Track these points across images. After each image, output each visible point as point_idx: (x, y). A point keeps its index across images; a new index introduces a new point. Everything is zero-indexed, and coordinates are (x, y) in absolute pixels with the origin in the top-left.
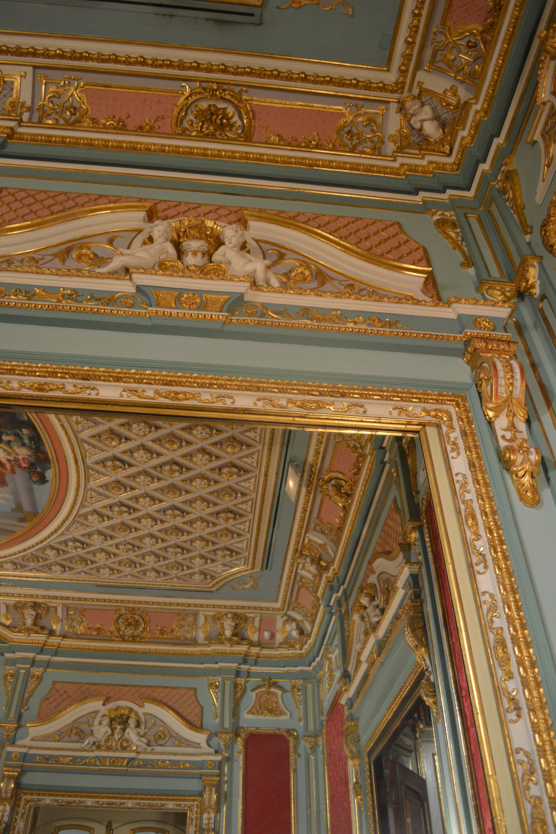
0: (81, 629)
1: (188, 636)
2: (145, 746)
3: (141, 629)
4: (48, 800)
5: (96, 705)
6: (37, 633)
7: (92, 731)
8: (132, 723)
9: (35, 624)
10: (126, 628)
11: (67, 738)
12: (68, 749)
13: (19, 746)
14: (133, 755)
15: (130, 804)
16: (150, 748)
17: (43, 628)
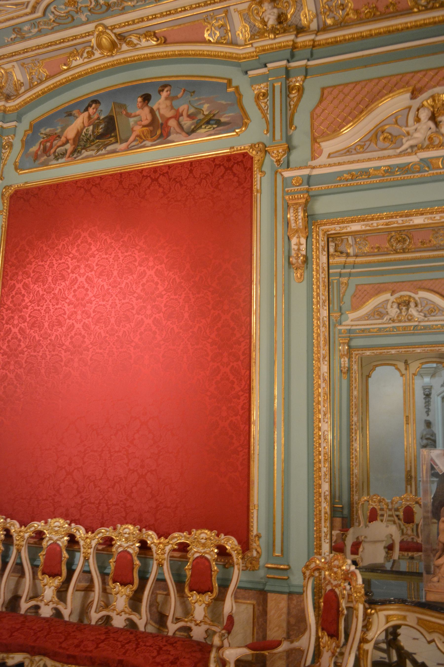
0: (366, 249)
2: (423, 318)
3: (407, 243)
4: (368, 353)
5: (387, 296)
6: (339, 256)
7: (387, 312)
8: (412, 304)
9: (336, 251)
10: (397, 244)
11: (372, 318)
12: (375, 324)
13: (344, 325)
14: (416, 323)
15: (419, 350)
16: (426, 319)
17: (342, 253)
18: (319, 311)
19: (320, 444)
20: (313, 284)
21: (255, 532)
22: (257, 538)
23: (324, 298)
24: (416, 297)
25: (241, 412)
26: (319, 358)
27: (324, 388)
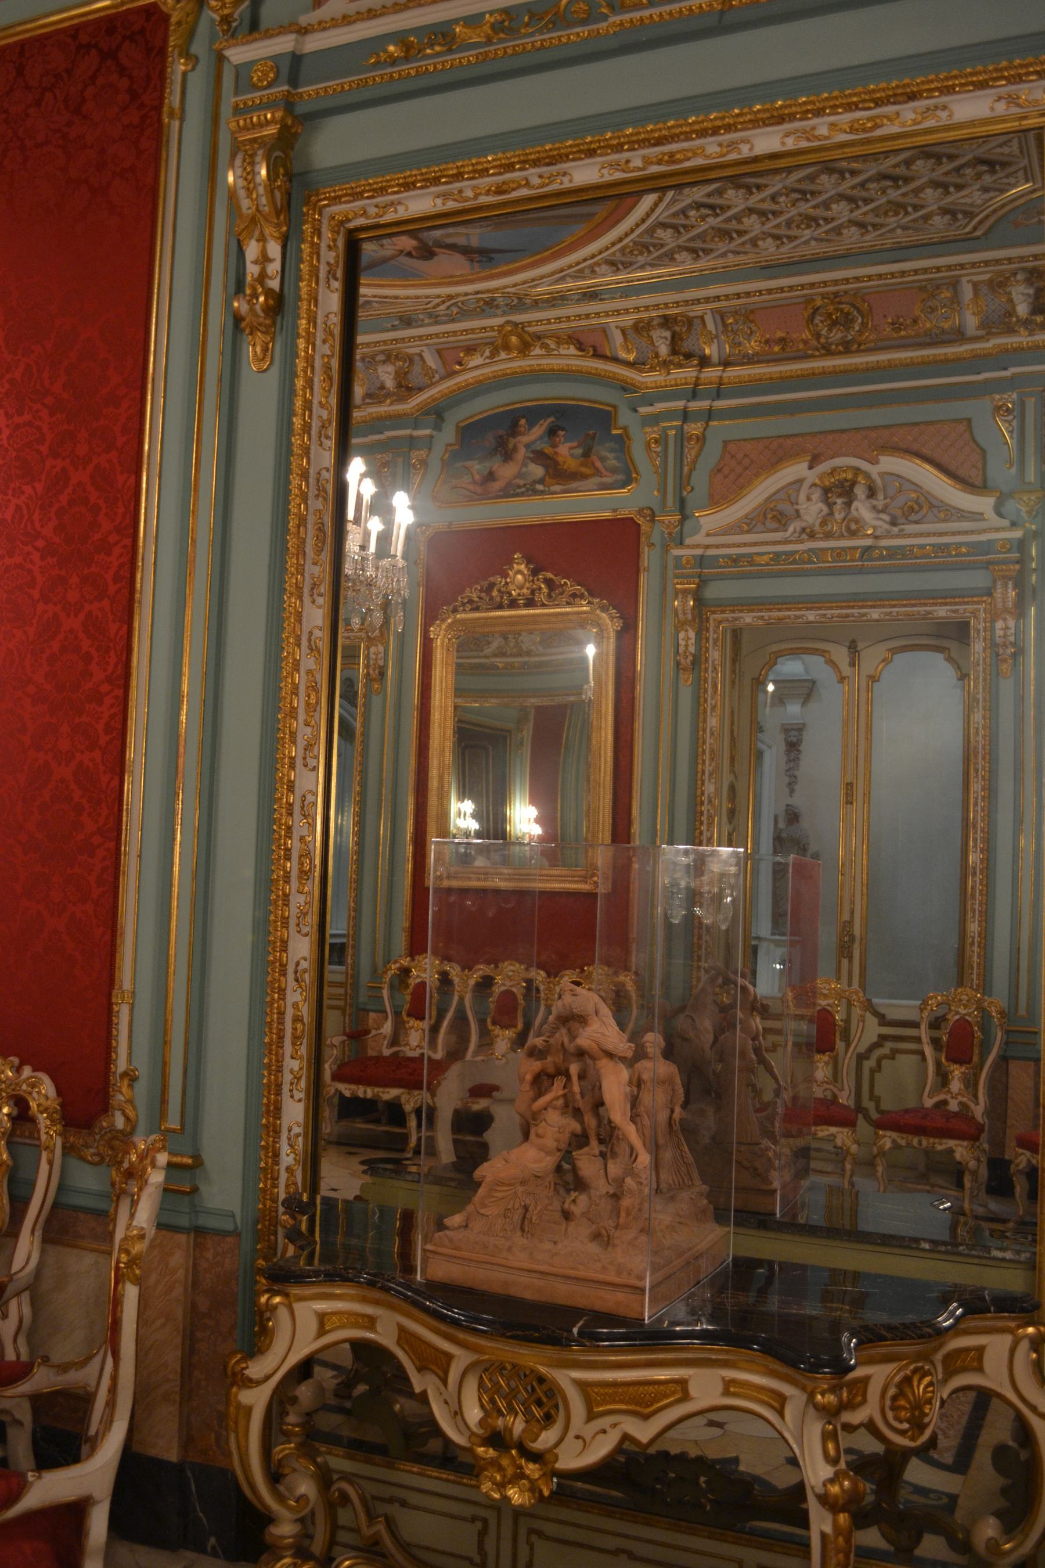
0: (752, 346)
1: (946, 326)
2: (887, 527)
3: (857, 328)
4: (748, 618)
5: (797, 470)
6: (681, 366)
7: (797, 511)
8: (860, 491)
9: (674, 352)
10: (830, 330)
11: (760, 527)
12: (765, 543)
13: (688, 547)
14: (869, 542)
15: (875, 614)
16: (896, 529)
17: (688, 356)
18: (307, 451)
19: (289, 829)
20: (297, 376)
21: (121, 1064)
22: (126, 1082)
23: (325, 414)
24: (873, 470)
25: (103, 740)
26: (299, 588)
27: (309, 672)
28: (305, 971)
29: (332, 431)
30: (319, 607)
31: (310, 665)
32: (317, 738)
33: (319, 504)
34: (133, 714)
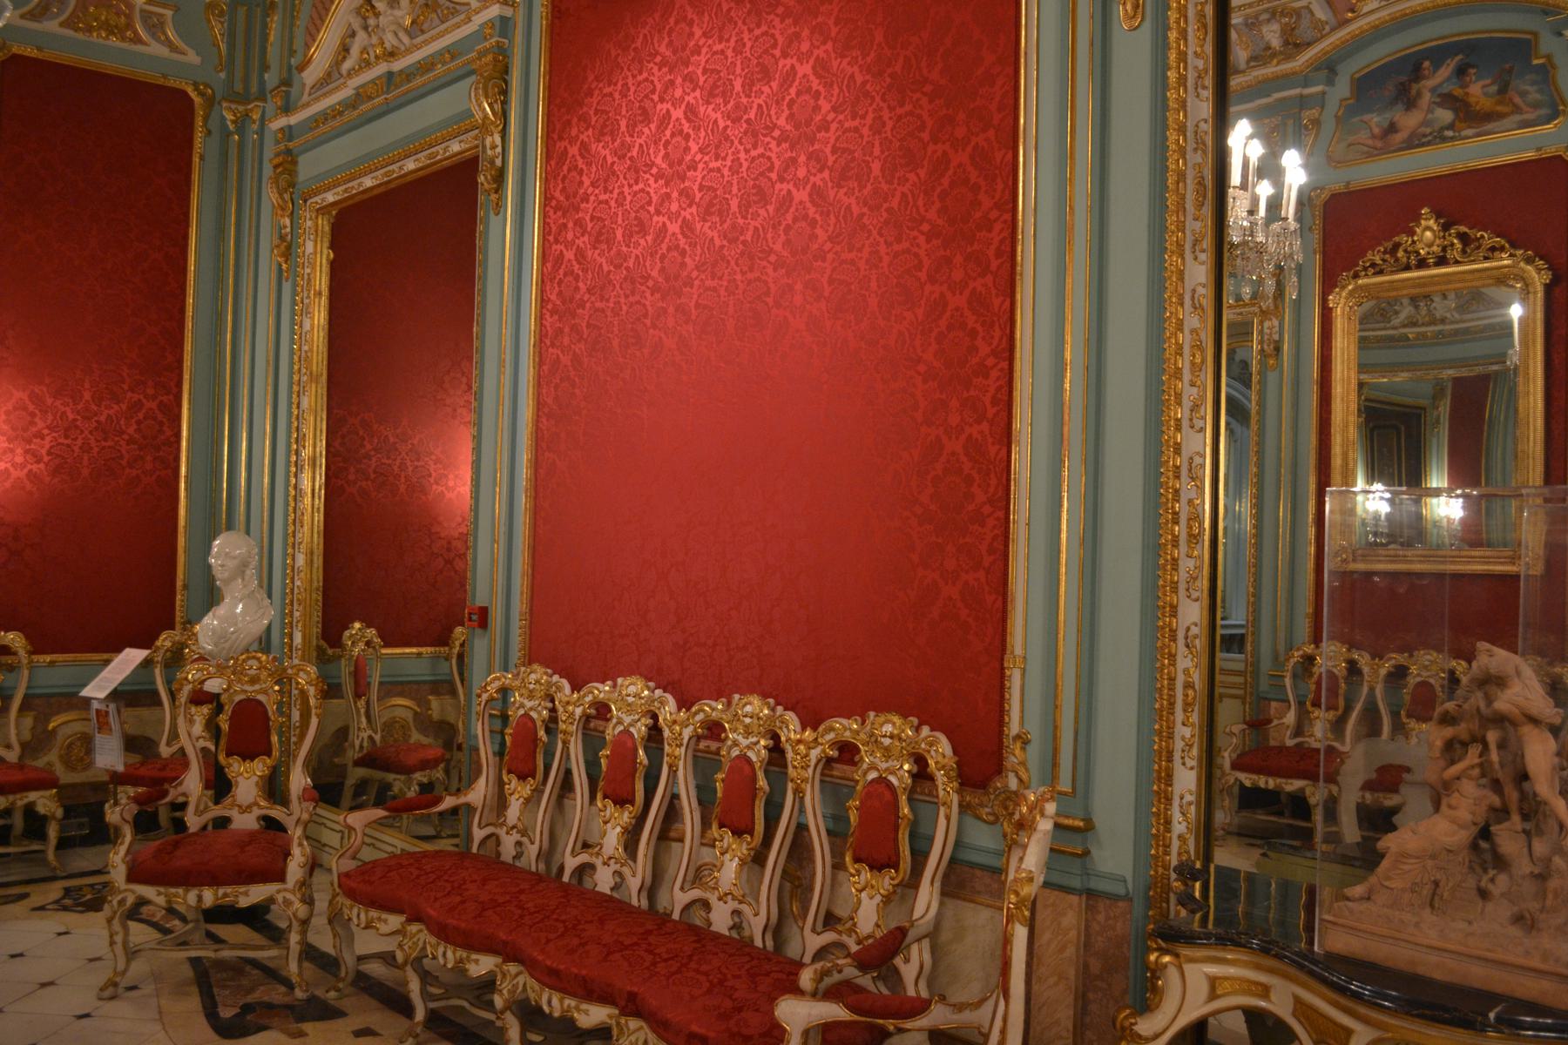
18: (1183, 104)
19: (1177, 492)
20: (1170, 29)
21: (1014, 727)
22: (1019, 744)
25: (991, 412)
26: (1180, 246)
27: (1193, 331)
28: (1196, 637)
29: (1209, 81)
30: (1202, 263)
31: (1194, 323)
32: (1203, 398)
33: (1198, 158)
34: (1017, 384)
